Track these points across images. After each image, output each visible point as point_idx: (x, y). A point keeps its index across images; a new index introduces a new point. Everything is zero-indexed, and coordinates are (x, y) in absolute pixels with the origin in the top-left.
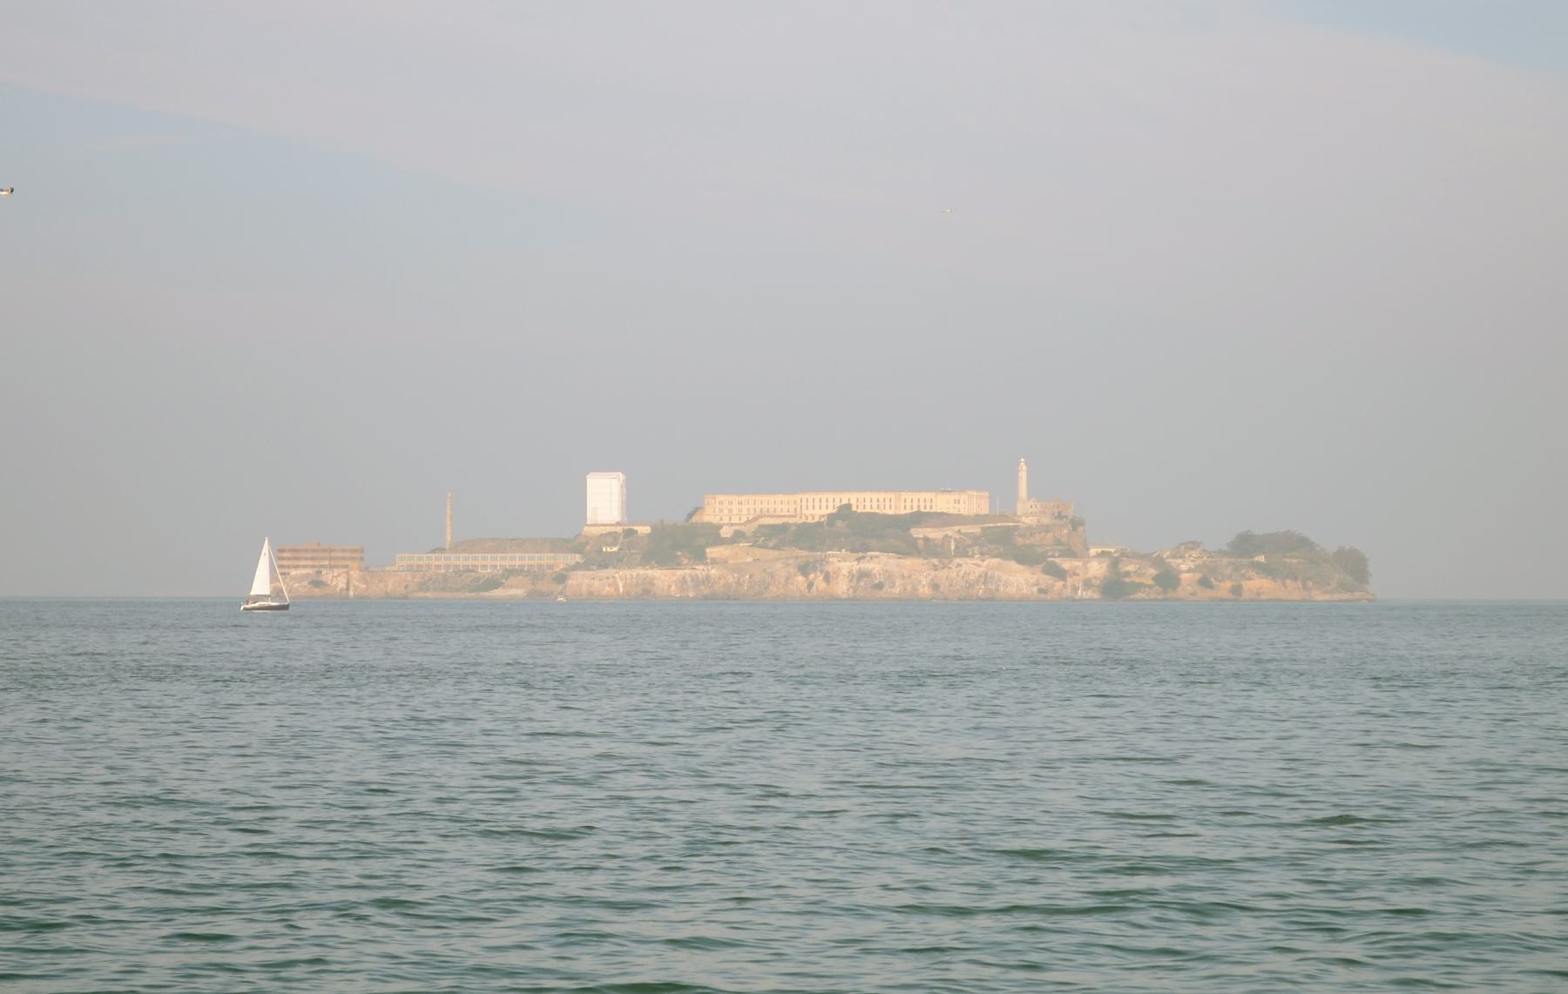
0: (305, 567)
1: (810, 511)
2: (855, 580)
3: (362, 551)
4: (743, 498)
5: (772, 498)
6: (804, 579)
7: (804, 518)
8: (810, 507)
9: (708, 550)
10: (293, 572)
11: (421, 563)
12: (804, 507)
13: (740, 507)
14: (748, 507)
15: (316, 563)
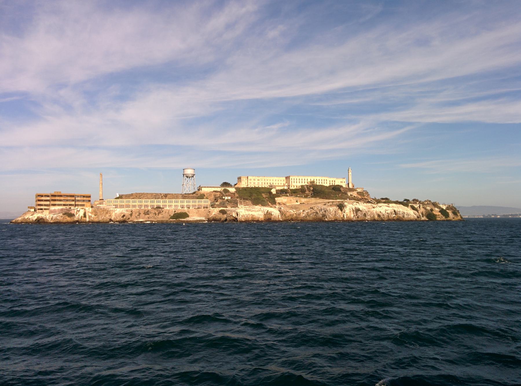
0: (59, 205)
1: (295, 184)
2: (355, 212)
3: (90, 197)
4: (259, 178)
5: (272, 178)
6: (341, 212)
7: (293, 186)
8: (295, 182)
9: (276, 199)
10: (52, 208)
11: (123, 204)
12: (293, 182)
13: (258, 181)
14: (262, 182)
15: (68, 203)
